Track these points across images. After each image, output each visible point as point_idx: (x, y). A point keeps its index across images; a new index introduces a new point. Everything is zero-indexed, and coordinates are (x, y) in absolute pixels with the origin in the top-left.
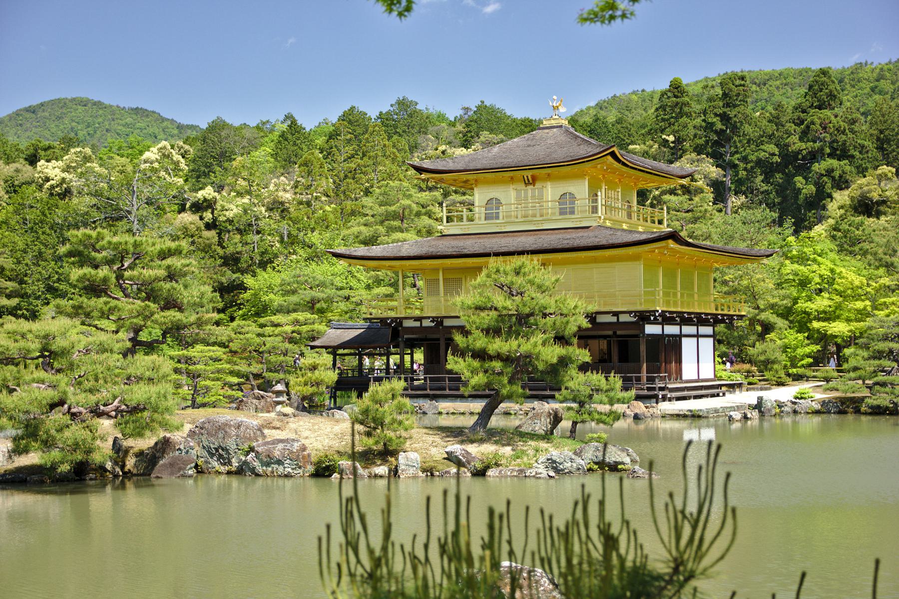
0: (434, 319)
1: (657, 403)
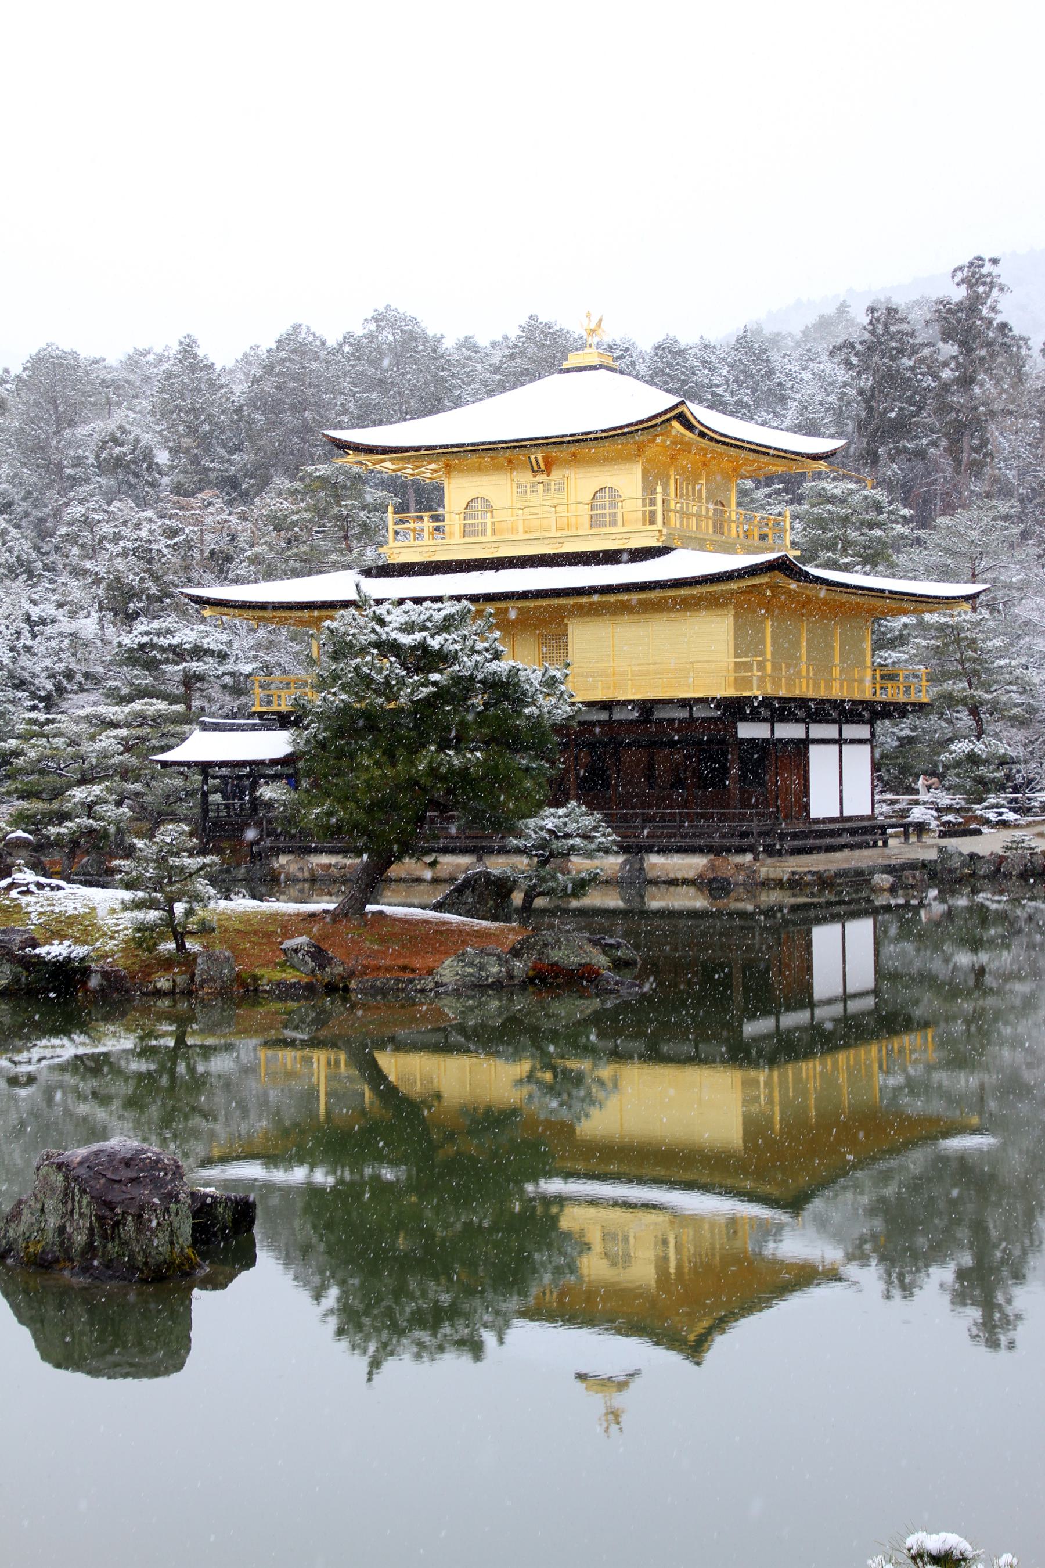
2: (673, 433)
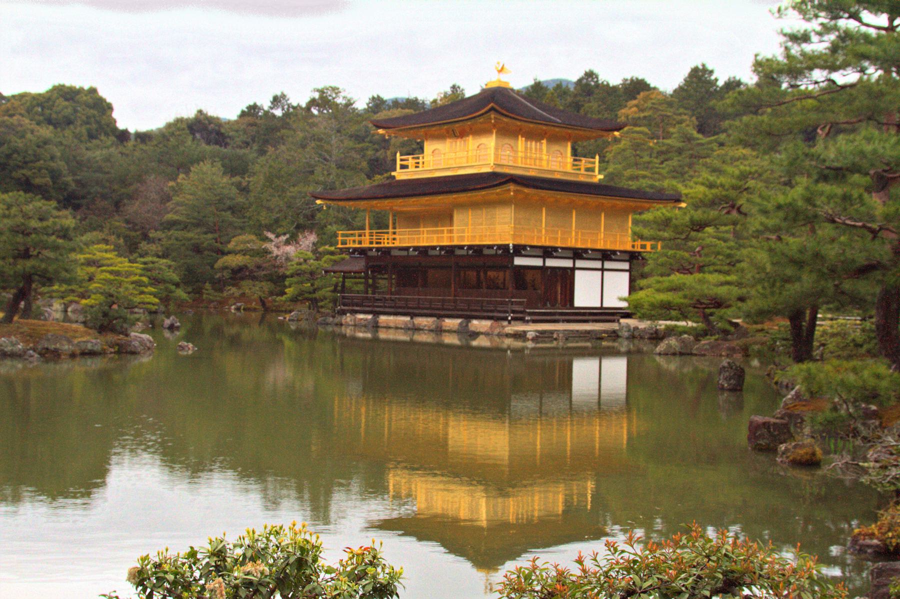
0: (378, 249)
1: (510, 322)
2: (493, 116)
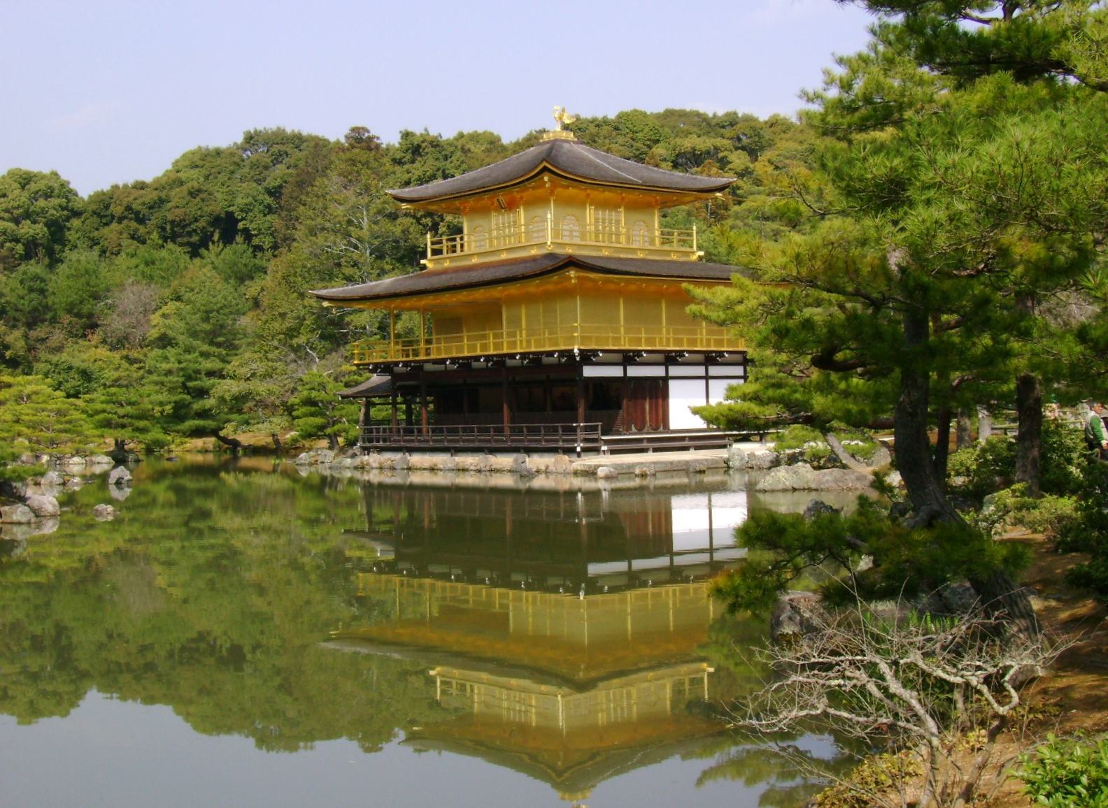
2: (546, 179)
